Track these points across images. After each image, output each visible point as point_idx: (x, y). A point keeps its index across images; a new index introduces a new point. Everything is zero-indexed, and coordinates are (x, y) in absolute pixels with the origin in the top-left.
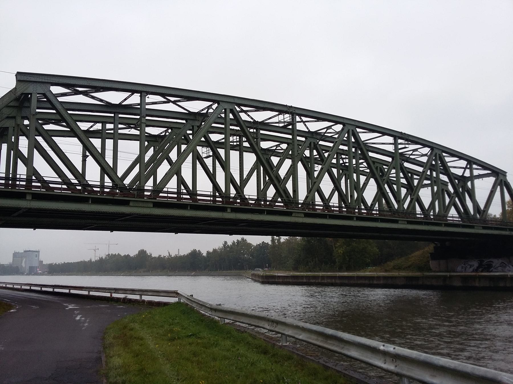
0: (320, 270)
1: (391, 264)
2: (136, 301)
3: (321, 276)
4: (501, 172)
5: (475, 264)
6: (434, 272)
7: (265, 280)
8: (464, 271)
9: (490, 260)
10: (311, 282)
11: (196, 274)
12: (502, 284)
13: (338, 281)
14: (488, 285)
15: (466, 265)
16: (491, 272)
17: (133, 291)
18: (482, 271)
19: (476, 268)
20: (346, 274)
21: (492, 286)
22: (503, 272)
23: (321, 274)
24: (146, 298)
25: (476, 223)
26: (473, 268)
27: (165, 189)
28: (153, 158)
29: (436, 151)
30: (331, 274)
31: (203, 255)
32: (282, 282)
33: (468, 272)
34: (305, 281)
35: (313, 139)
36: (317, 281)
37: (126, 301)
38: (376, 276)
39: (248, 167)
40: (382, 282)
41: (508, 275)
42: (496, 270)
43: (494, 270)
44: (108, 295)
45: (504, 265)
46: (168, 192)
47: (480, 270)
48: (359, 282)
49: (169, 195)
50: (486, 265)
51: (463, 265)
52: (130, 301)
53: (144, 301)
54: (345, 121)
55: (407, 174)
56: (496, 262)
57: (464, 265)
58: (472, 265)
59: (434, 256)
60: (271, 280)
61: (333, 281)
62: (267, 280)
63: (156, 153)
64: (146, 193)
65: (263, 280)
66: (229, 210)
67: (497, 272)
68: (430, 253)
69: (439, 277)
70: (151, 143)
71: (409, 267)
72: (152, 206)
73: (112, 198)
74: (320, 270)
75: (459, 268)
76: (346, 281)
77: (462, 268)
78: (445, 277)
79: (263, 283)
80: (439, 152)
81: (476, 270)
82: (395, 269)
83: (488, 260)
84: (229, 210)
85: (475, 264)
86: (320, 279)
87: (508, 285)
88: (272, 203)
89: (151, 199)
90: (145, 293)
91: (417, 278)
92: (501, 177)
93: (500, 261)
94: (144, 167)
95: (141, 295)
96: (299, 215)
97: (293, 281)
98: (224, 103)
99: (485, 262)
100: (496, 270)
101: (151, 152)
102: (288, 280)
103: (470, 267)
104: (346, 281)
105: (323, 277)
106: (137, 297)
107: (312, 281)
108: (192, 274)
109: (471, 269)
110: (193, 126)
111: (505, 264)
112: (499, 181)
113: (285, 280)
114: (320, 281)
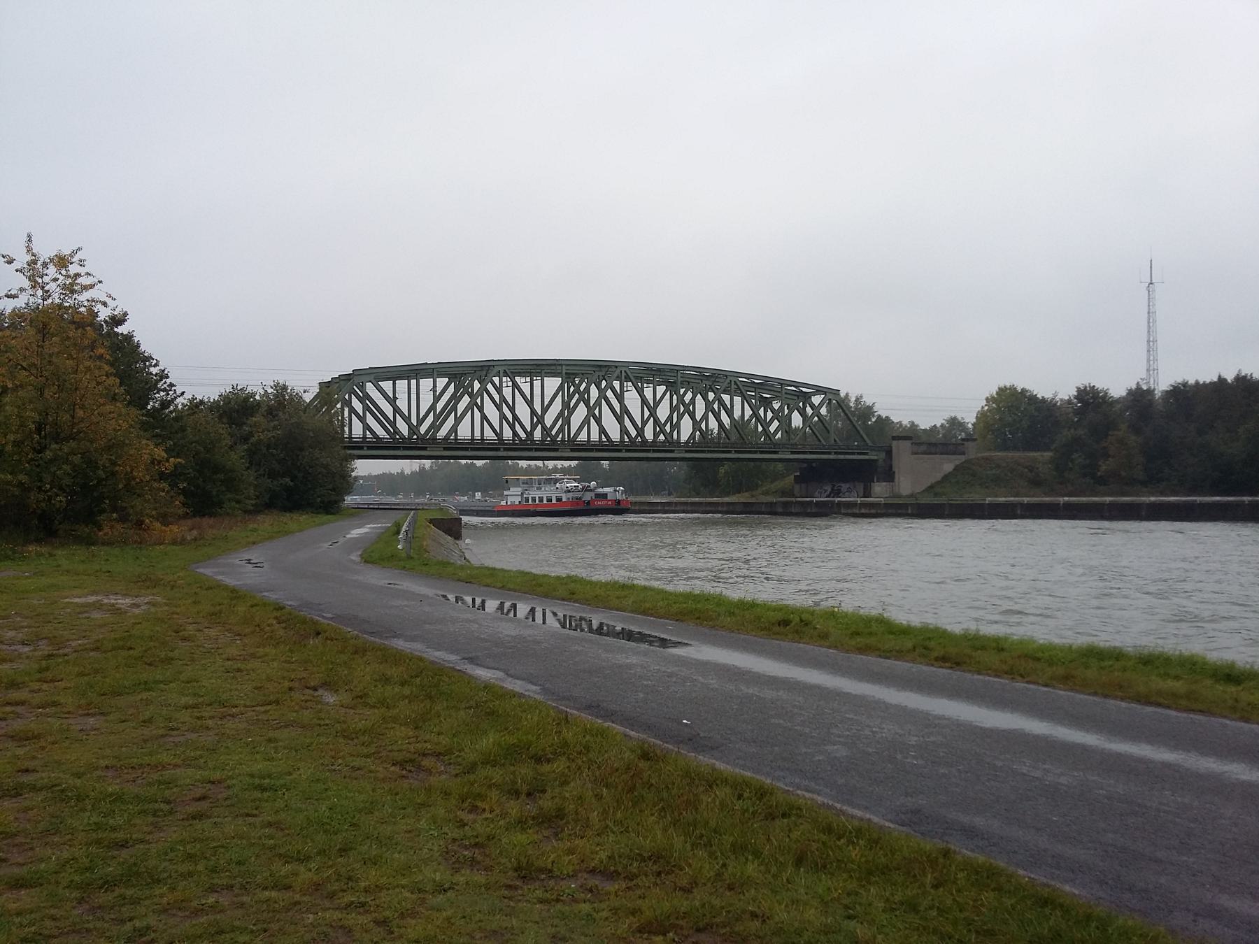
0: (698, 495)
13: (689, 508)
28: (453, 397)
29: (729, 378)
34: (660, 508)
39: (549, 393)
40: (725, 509)
56: (844, 487)
59: (798, 480)
63: (456, 390)
80: (733, 379)
87: (813, 511)
93: (848, 485)
94: (436, 417)
107: (666, 508)
113: (642, 508)
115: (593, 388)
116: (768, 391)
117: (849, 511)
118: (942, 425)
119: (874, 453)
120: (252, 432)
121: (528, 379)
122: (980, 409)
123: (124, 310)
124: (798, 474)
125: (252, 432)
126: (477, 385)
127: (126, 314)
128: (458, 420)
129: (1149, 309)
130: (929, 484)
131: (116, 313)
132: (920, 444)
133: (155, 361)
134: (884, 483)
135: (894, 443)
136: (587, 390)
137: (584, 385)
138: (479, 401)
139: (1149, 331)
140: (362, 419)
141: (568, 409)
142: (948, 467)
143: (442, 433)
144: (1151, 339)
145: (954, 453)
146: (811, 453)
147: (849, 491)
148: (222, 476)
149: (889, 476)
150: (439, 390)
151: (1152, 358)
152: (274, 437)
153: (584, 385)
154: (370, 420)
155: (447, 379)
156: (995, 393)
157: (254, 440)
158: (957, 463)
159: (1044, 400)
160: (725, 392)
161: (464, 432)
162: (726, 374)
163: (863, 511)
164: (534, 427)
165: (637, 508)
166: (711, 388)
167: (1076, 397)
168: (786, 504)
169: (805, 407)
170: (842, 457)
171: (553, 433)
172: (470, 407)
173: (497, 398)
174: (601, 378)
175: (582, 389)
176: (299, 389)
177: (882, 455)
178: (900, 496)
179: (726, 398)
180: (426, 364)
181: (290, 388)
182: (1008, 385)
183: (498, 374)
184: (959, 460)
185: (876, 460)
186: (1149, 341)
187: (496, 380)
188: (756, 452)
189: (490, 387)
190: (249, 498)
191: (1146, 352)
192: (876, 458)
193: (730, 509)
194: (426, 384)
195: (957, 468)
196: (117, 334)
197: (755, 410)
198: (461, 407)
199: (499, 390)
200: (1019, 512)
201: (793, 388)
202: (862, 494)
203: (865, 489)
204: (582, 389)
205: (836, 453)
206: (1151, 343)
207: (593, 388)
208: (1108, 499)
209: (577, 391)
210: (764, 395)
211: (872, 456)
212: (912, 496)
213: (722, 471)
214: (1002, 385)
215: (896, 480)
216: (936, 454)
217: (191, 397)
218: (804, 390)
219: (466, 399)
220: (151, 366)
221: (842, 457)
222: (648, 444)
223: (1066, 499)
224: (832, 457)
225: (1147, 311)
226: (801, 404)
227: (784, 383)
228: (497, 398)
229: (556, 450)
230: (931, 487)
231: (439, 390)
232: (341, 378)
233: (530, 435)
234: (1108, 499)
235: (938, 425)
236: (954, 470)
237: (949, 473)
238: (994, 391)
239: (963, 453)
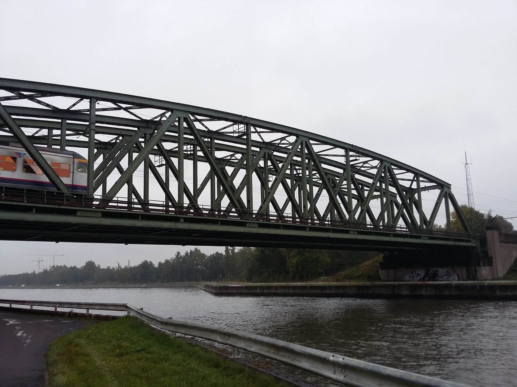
0: (274, 280)
1: (343, 273)
2: (82, 315)
3: (275, 286)
4: (446, 185)
5: (422, 273)
6: (384, 281)
7: (219, 291)
8: (411, 280)
9: (435, 269)
10: (265, 293)
12: (447, 293)
14: (434, 294)
15: (414, 274)
16: (437, 280)
17: (79, 305)
18: (428, 280)
19: (423, 277)
20: (299, 284)
21: (438, 294)
22: (448, 281)
23: (275, 284)
24: (93, 312)
25: (422, 234)
26: (420, 276)
27: (115, 199)
28: (102, 166)
29: (385, 163)
30: (284, 284)
31: (155, 266)
32: (236, 293)
33: (415, 281)
35: (266, 149)
36: (270, 292)
37: (71, 316)
38: (328, 285)
40: (333, 292)
41: (452, 284)
42: (442, 279)
43: (440, 279)
44: (52, 309)
45: (449, 274)
46: (118, 202)
47: (427, 278)
48: (312, 292)
49: (119, 205)
50: (431, 274)
52: (76, 315)
53: (91, 315)
54: (299, 133)
55: (358, 185)
56: (442, 271)
57: (412, 274)
58: (419, 274)
59: (383, 266)
60: (225, 291)
61: (287, 291)
64: (95, 203)
65: (216, 291)
66: (182, 220)
67: (443, 281)
68: (380, 263)
69: (388, 286)
70: (101, 150)
71: (360, 276)
72: (100, 215)
73: (57, 207)
74: (274, 280)
75: (407, 277)
77: (410, 277)
78: (394, 286)
79: (217, 294)
80: (388, 165)
81: (423, 279)
82: (346, 279)
83: (435, 269)
84: (182, 220)
85: (422, 273)
86: (274, 289)
88: (226, 214)
89: (100, 208)
90: (93, 307)
91: (367, 287)
92: (446, 189)
93: (445, 270)
95: (88, 309)
96: (254, 226)
97: (247, 292)
98: (178, 112)
99: (431, 271)
100: (442, 279)
101: (100, 160)
102: (242, 291)
103: (417, 276)
105: (276, 288)
106: (83, 311)
107: (266, 291)
108: (143, 286)
109: (418, 278)
110: (145, 134)
111: (450, 273)
112: (444, 193)
113: (239, 291)
114: (273, 291)
119: (473, 241)
134: (488, 268)
147: (448, 274)
149: (489, 261)
170: (457, 243)
177: (479, 243)
185: (473, 247)
192: (474, 245)
202: (465, 276)
206: (469, 195)
215: (494, 264)
216: (508, 243)
221: (457, 243)
224: (451, 243)
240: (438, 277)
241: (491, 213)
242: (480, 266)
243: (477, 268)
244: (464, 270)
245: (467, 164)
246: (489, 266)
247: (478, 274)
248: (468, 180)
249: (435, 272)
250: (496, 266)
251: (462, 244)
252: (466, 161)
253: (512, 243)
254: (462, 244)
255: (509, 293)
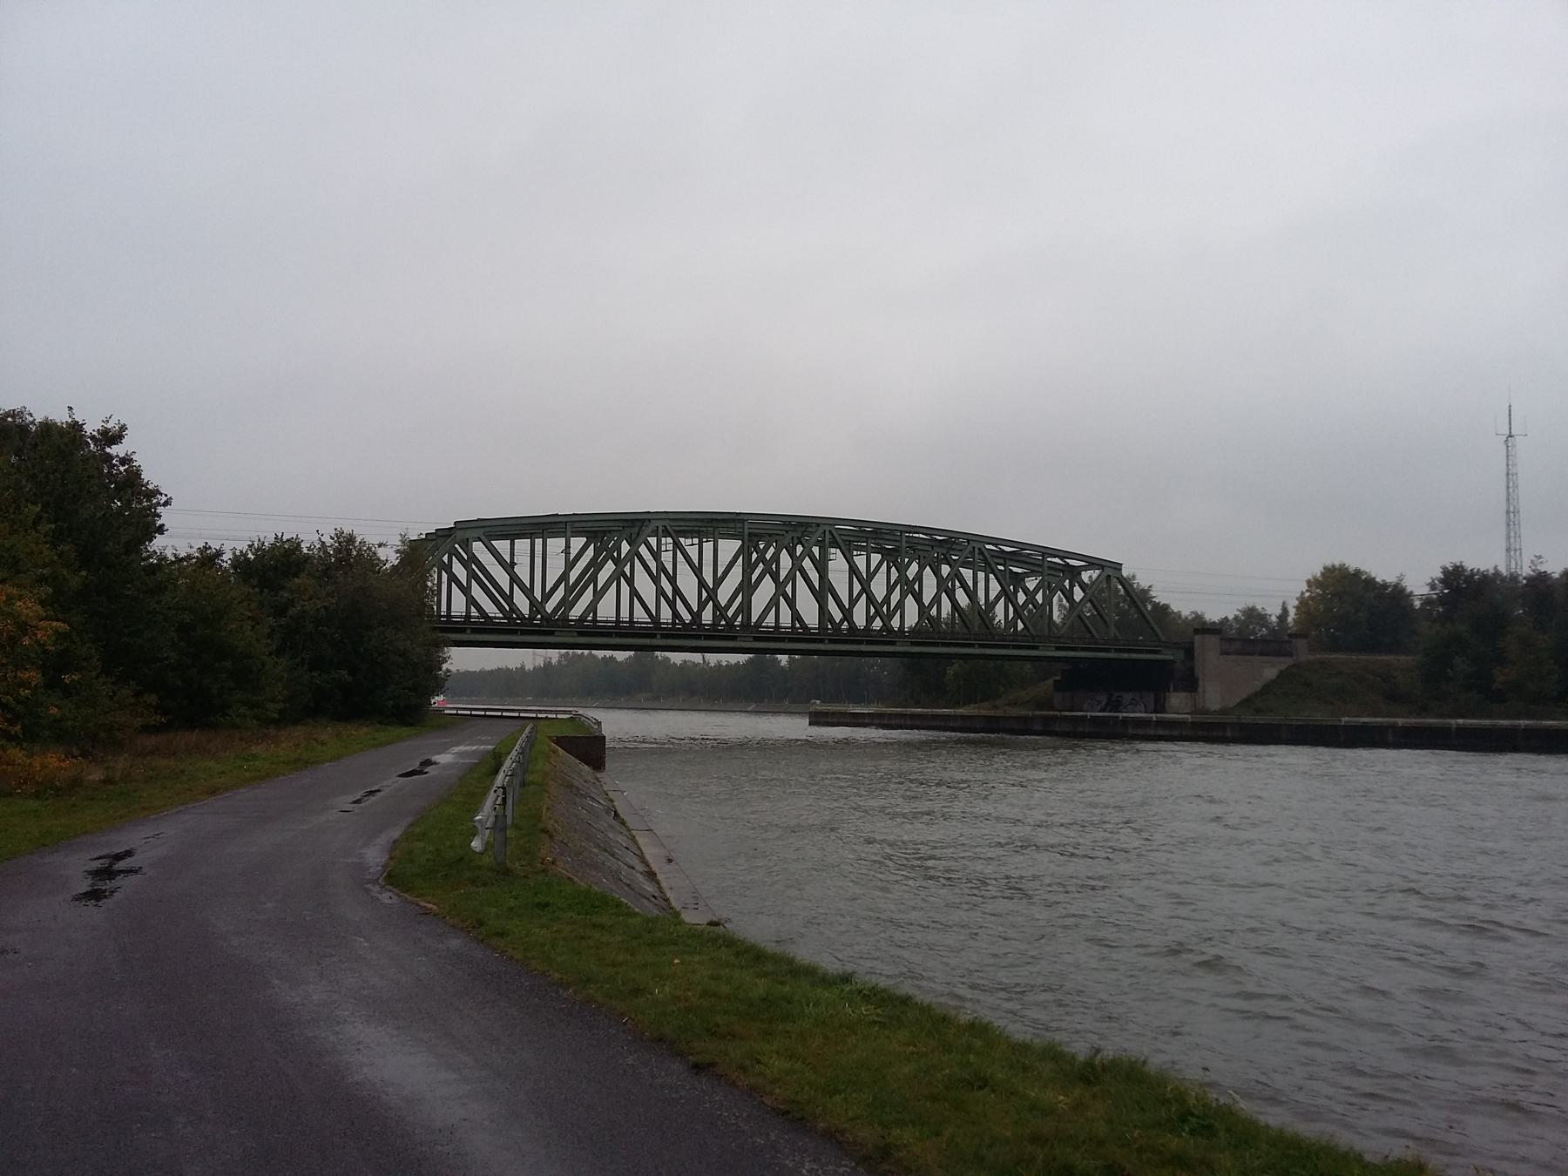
0: (918, 704)
5: (1103, 699)
11: (757, 709)
18: (1110, 712)
22: (1145, 713)
29: (972, 543)
31: (782, 664)
34: (867, 721)
38: (953, 713)
40: (958, 724)
43: (1124, 710)
44: (534, 715)
47: (1109, 708)
48: (934, 723)
51: (1090, 701)
56: (1127, 697)
59: (1058, 686)
61: (903, 722)
62: (817, 719)
63: (597, 553)
66: (659, 636)
71: (1028, 702)
75: (1086, 706)
76: (918, 722)
80: (977, 545)
84: (659, 636)
85: (1103, 699)
91: (997, 718)
94: (569, 590)
104: (918, 722)
106: (554, 716)
108: (749, 709)
109: (1099, 708)
115: (784, 555)
116: (1020, 563)
117: (1141, 732)
118: (1236, 618)
120: (293, 600)
121: (696, 541)
122: (1298, 595)
123: (122, 423)
124: (1057, 678)
125: (293, 600)
126: (625, 547)
127: (123, 428)
128: (598, 595)
129: (1508, 470)
130: (1244, 697)
131: (109, 426)
132: (1231, 640)
133: (164, 498)
134: (1184, 694)
135: (1197, 638)
136: (776, 558)
137: (772, 550)
138: (627, 569)
139: (1508, 500)
140: (466, 591)
141: (747, 588)
142: (1270, 673)
143: (576, 612)
144: (1511, 509)
145: (1278, 654)
146: (1084, 649)
148: (228, 664)
149: (1190, 683)
150: (574, 552)
151: (1512, 534)
152: (325, 608)
153: (772, 550)
154: (476, 591)
155: (585, 539)
156: (1319, 574)
157: (292, 611)
158: (1283, 667)
159: (1385, 586)
160: (966, 565)
161: (606, 610)
162: (971, 538)
163: (1161, 732)
164: (702, 605)
165: (835, 720)
166: (945, 558)
167: (1441, 581)
168: (1045, 719)
169: (1072, 586)
170: (1125, 656)
171: (730, 613)
172: (617, 576)
173: (653, 565)
174: (796, 541)
175: (768, 556)
176: (372, 540)
177: (1181, 655)
178: (1207, 712)
179: (967, 573)
180: (557, 515)
181: (358, 540)
182: (1337, 564)
183: (655, 533)
184: (1284, 663)
186: (1508, 512)
187: (653, 541)
188: (1007, 647)
189: (643, 550)
190: (273, 700)
191: (1505, 525)
192: (1172, 658)
193: (966, 724)
194: (556, 544)
195: (1281, 674)
196: (110, 457)
197: (1005, 586)
198: (603, 577)
199: (656, 555)
200: (1391, 739)
201: (1057, 560)
202: (1151, 706)
203: (1156, 701)
204: (768, 556)
205: (1116, 650)
206: (1512, 515)
207: (784, 555)
208: (1523, 723)
209: (761, 559)
210: (1015, 570)
211: (1167, 656)
212: (1224, 711)
213: (950, 672)
214: (1328, 563)
215: (1200, 690)
217: (201, 545)
218: (1072, 562)
219: (610, 567)
220: (158, 504)
221: (1125, 656)
222: (858, 632)
223: (1460, 721)
225: (1505, 472)
226: (1067, 583)
227: (1046, 552)
228: (653, 565)
229: (734, 638)
230: (1247, 701)
231: (574, 552)
232: (439, 533)
233: (696, 616)
234: (1523, 723)
235: (1231, 617)
236: (1278, 677)
237: (1273, 681)
238: (1316, 570)
239: (1290, 655)
240: (1122, 707)
241: (1402, 583)
242: (1169, 691)
243: (1167, 694)
244: (1152, 696)
245: (1511, 436)
246: (1184, 691)
247: (1167, 705)
248: (1510, 477)
249: (1120, 699)
250: (1204, 692)
251: (1134, 656)
252: (1510, 428)
253: (1262, 654)
254: (1134, 656)
255: (1141, 732)
